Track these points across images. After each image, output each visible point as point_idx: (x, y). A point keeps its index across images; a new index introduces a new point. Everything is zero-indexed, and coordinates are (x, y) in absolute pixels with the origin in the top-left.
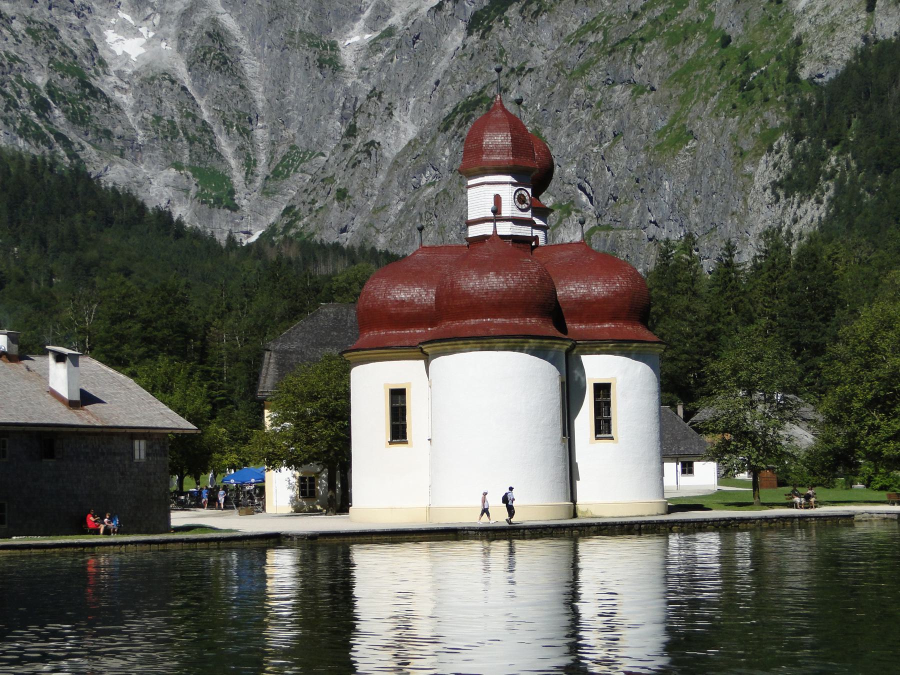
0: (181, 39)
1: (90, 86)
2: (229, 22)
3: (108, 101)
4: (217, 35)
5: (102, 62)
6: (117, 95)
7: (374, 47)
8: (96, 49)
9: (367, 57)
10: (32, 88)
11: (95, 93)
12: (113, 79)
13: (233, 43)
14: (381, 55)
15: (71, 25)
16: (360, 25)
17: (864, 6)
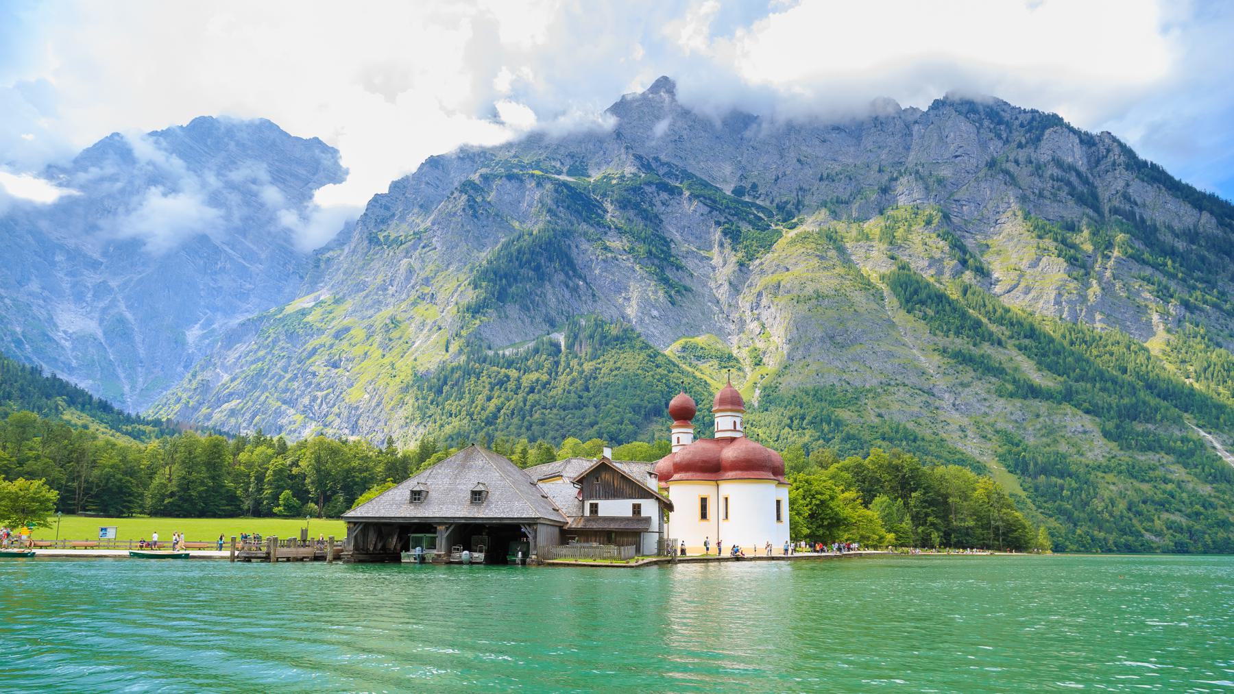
0: (101, 321)
1: (48, 335)
2: (129, 316)
3: (58, 344)
4: (121, 321)
5: (55, 325)
6: (63, 341)
7: (204, 337)
8: (52, 318)
9: (200, 341)
10: (13, 334)
11: (50, 339)
12: (61, 334)
13: (130, 325)
14: (207, 341)
15: (39, 305)
16: (197, 326)
17: (444, 349)
